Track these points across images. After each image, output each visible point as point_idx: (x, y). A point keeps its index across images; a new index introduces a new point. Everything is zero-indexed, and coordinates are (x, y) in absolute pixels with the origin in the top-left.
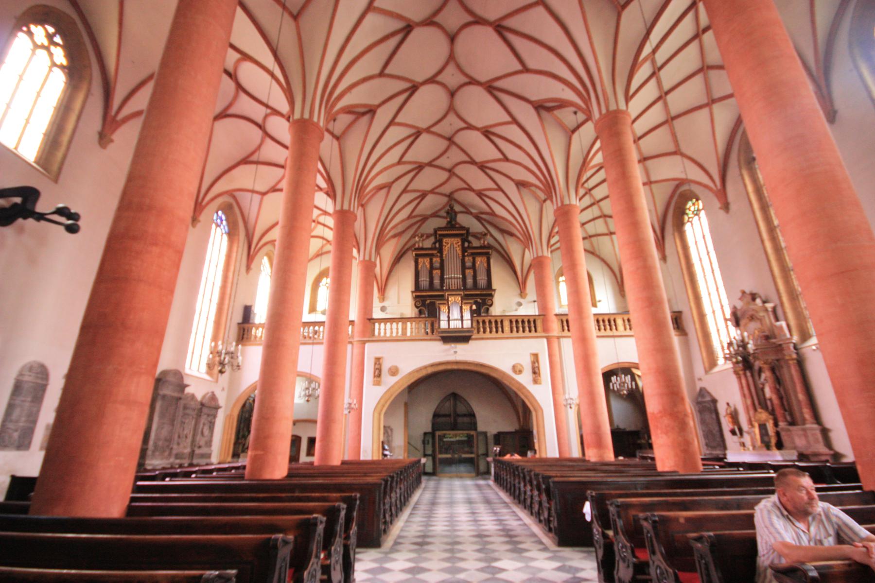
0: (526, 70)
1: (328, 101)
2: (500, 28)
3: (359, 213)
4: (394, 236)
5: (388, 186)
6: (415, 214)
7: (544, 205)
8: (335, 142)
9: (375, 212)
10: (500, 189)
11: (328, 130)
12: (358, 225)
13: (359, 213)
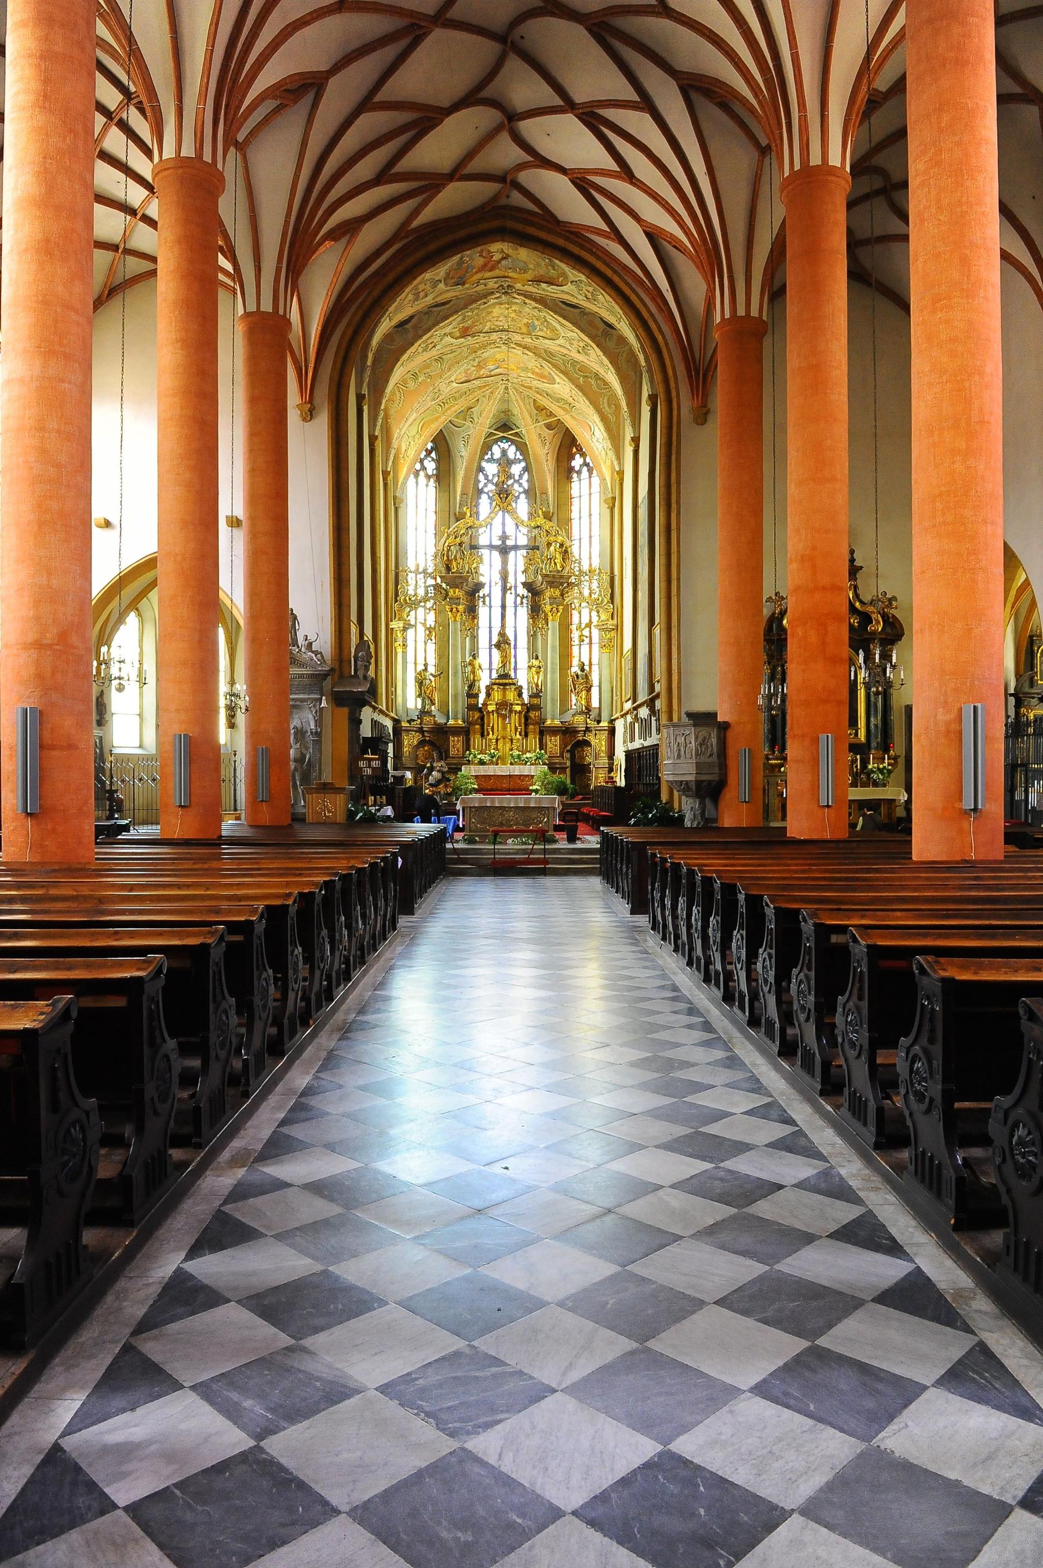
4: (335, 235)
6: (399, 168)
7: (767, 161)
9: (276, 166)
10: (647, 104)
12: (229, 208)
13: (230, 166)
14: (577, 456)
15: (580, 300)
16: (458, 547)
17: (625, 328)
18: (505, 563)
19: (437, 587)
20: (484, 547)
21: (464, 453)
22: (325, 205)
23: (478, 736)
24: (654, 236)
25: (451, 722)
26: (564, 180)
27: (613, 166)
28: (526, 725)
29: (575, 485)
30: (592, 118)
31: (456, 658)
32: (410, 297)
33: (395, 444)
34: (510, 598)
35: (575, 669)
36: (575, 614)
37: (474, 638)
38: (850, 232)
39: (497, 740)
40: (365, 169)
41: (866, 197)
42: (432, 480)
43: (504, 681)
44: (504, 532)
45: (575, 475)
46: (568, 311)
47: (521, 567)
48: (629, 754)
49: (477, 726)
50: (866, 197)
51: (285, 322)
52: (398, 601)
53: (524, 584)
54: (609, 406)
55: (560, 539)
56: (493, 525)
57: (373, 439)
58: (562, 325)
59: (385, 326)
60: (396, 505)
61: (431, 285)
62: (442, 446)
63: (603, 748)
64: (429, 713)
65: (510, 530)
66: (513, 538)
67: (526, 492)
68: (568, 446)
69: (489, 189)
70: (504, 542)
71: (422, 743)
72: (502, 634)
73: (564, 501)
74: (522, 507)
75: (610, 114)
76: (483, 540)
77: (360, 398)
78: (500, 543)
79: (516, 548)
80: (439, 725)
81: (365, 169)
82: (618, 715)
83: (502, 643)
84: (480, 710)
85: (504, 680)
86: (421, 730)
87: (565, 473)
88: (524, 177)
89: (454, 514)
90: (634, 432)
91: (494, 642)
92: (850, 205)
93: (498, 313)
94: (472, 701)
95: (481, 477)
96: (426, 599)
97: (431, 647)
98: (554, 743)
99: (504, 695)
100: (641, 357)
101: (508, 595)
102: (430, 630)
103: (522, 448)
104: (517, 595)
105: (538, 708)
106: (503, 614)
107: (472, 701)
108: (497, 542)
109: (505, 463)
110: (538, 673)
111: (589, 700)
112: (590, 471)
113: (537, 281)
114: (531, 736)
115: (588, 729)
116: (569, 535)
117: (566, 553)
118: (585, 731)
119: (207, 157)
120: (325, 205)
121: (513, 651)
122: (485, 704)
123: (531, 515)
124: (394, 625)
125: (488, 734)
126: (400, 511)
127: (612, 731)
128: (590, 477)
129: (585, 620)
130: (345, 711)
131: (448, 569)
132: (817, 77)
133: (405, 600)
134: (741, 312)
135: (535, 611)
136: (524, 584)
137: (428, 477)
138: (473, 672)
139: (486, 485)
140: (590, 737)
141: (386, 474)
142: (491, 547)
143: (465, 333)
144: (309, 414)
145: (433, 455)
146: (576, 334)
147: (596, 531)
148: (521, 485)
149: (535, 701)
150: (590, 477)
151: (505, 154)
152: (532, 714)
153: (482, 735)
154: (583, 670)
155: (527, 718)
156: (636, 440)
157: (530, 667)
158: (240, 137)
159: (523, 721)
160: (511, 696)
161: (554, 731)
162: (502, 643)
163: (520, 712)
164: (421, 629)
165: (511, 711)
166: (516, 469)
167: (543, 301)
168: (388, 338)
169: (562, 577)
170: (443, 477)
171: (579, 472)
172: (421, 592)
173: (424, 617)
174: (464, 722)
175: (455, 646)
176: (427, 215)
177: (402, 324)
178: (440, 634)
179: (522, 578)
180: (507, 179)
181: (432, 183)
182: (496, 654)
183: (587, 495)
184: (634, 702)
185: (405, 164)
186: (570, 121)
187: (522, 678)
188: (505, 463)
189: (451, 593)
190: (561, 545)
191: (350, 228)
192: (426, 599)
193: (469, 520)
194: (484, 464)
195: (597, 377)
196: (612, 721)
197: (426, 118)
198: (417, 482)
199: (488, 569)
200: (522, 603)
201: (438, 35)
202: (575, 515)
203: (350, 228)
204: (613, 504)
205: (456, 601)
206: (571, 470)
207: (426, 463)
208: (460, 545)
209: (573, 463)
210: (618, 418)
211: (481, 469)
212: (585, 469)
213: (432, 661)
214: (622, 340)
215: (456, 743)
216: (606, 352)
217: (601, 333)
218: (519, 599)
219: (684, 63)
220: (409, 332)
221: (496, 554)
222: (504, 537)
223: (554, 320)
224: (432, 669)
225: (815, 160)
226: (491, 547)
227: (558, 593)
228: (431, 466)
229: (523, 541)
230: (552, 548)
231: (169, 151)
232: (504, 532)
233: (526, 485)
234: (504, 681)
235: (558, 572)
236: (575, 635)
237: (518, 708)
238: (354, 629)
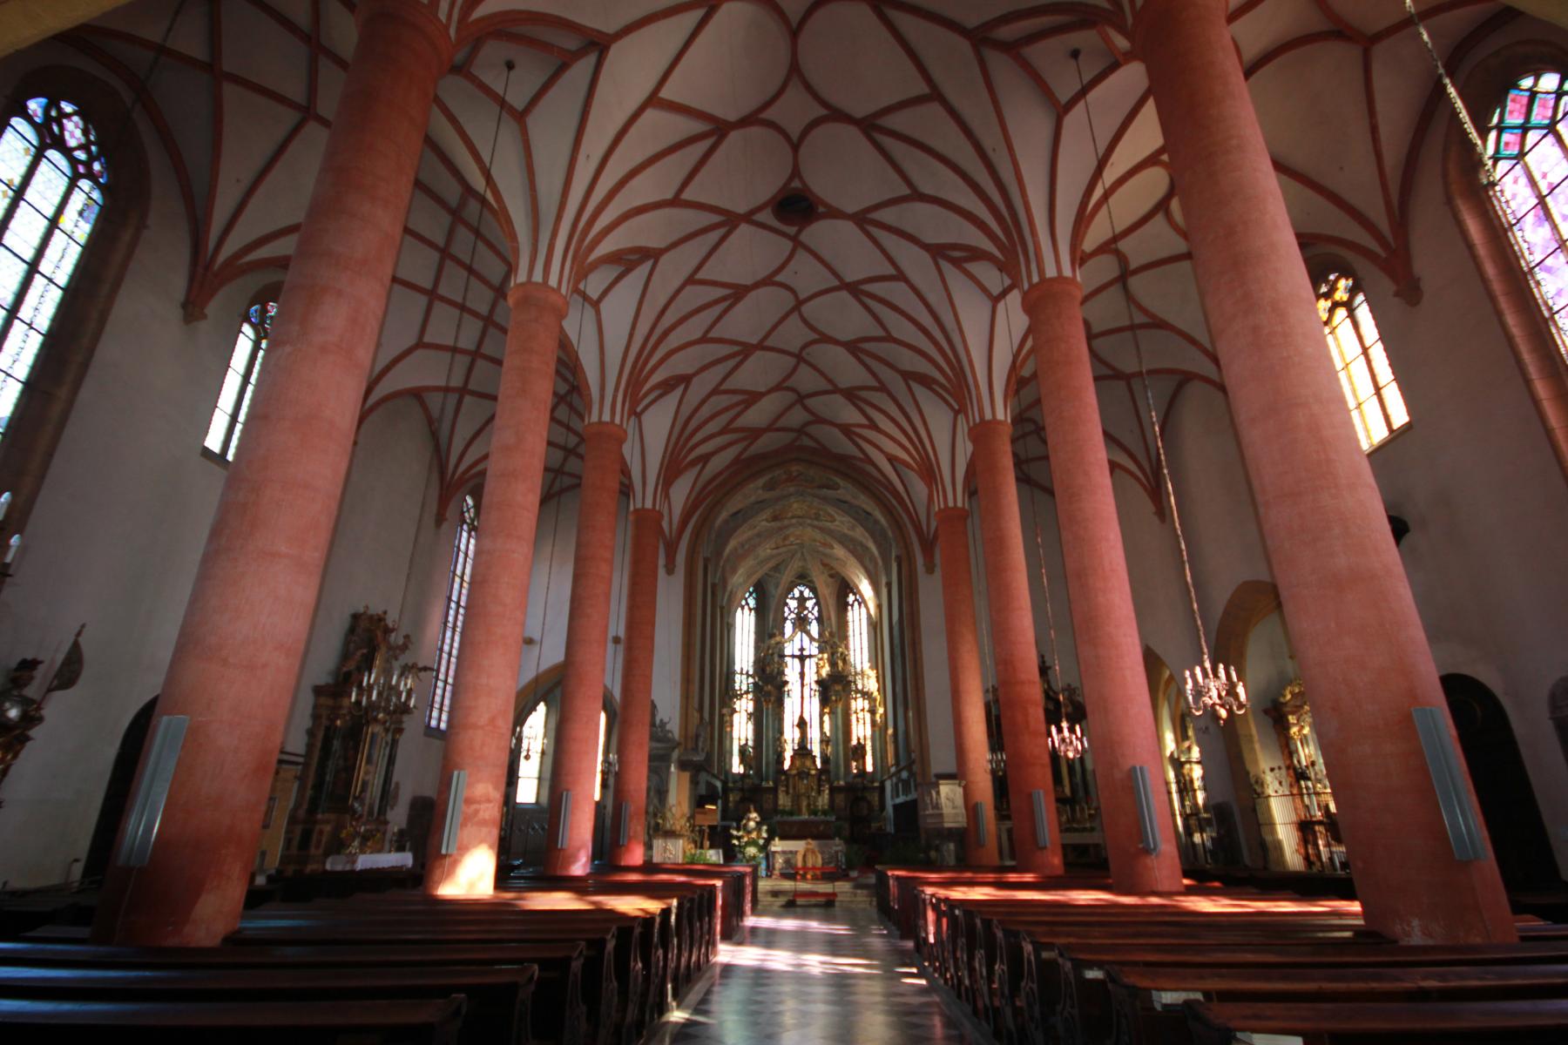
0: (918, 196)
1: (582, 240)
2: (869, 126)
3: (631, 427)
4: (693, 463)
5: (685, 380)
8: (589, 312)
10: (883, 388)
11: (576, 290)
13: (631, 427)
15: (848, 498)
17: (878, 515)
19: (755, 684)
21: (775, 593)
22: (691, 444)
24: (892, 459)
26: (836, 431)
27: (864, 421)
29: (850, 614)
30: (851, 395)
31: (769, 734)
34: (806, 690)
35: (854, 742)
38: (1015, 455)
40: (712, 427)
41: (1024, 436)
46: (840, 504)
47: (814, 669)
48: (895, 807)
50: (1024, 436)
51: (661, 515)
52: (729, 695)
53: (817, 682)
56: (794, 642)
57: (714, 586)
59: (724, 515)
60: (729, 627)
61: (753, 491)
62: (761, 592)
68: (845, 588)
69: (793, 435)
73: (843, 624)
74: (814, 628)
75: (863, 394)
76: (788, 652)
77: (706, 561)
78: (797, 653)
79: (810, 656)
81: (712, 427)
83: (802, 724)
85: (803, 751)
86: (742, 790)
87: (843, 607)
88: (812, 429)
89: (768, 634)
92: (1014, 441)
93: (797, 507)
96: (747, 692)
97: (751, 726)
100: (890, 534)
102: (750, 715)
103: (813, 590)
106: (801, 703)
108: (797, 653)
109: (802, 600)
113: (821, 487)
115: (865, 788)
116: (847, 647)
117: (845, 661)
119: (617, 421)
120: (691, 444)
123: (820, 634)
124: (725, 711)
127: (882, 789)
130: (687, 775)
131: (763, 670)
132: (985, 372)
134: (951, 504)
135: (825, 701)
136: (817, 682)
140: (868, 795)
141: (722, 608)
142: (793, 656)
143: (775, 518)
144: (670, 570)
146: (846, 519)
151: (797, 417)
155: (819, 780)
156: (889, 585)
158: (639, 409)
160: (808, 763)
161: (840, 789)
162: (802, 724)
164: (744, 715)
166: (810, 604)
167: (825, 499)
168: (726, 522)
170: (760, 612)
172: (744, 688)
173: (744, 706)
176: (753, 450)
177: (736, 513)
178: (757, 717)
180: (801, 431)
181: (755, 433)
182: (797, 731)
183: (858, 621)
185: (739, 423)
186: (839, 399)
187: (816, 751)
188: (802, 600)
191: (705, 459)
192: (747, 692)
193: (778, 639)
195: (862, 545)
197: (753, 398)
199: (791, 671)
201: (759, 353)
202: (850, 633)
203: (705, 459)
204: (874, 626)
205: (769, 694)
206: (847, 604)
213: (750, 736)
214: (876, 522)
216: (867, 530)
217: (863, 518)
219: (908, 367)
220: (740, 517)
221: (797, 661)
222: (802, 649)
223: (831, 510)
224: (750, 743)
225: (988, 416)
226: (793, 656)
228: (752, 602)
229: (815, 651)
231: (594, 418)
236: (854, 718)
238: (696, 715)
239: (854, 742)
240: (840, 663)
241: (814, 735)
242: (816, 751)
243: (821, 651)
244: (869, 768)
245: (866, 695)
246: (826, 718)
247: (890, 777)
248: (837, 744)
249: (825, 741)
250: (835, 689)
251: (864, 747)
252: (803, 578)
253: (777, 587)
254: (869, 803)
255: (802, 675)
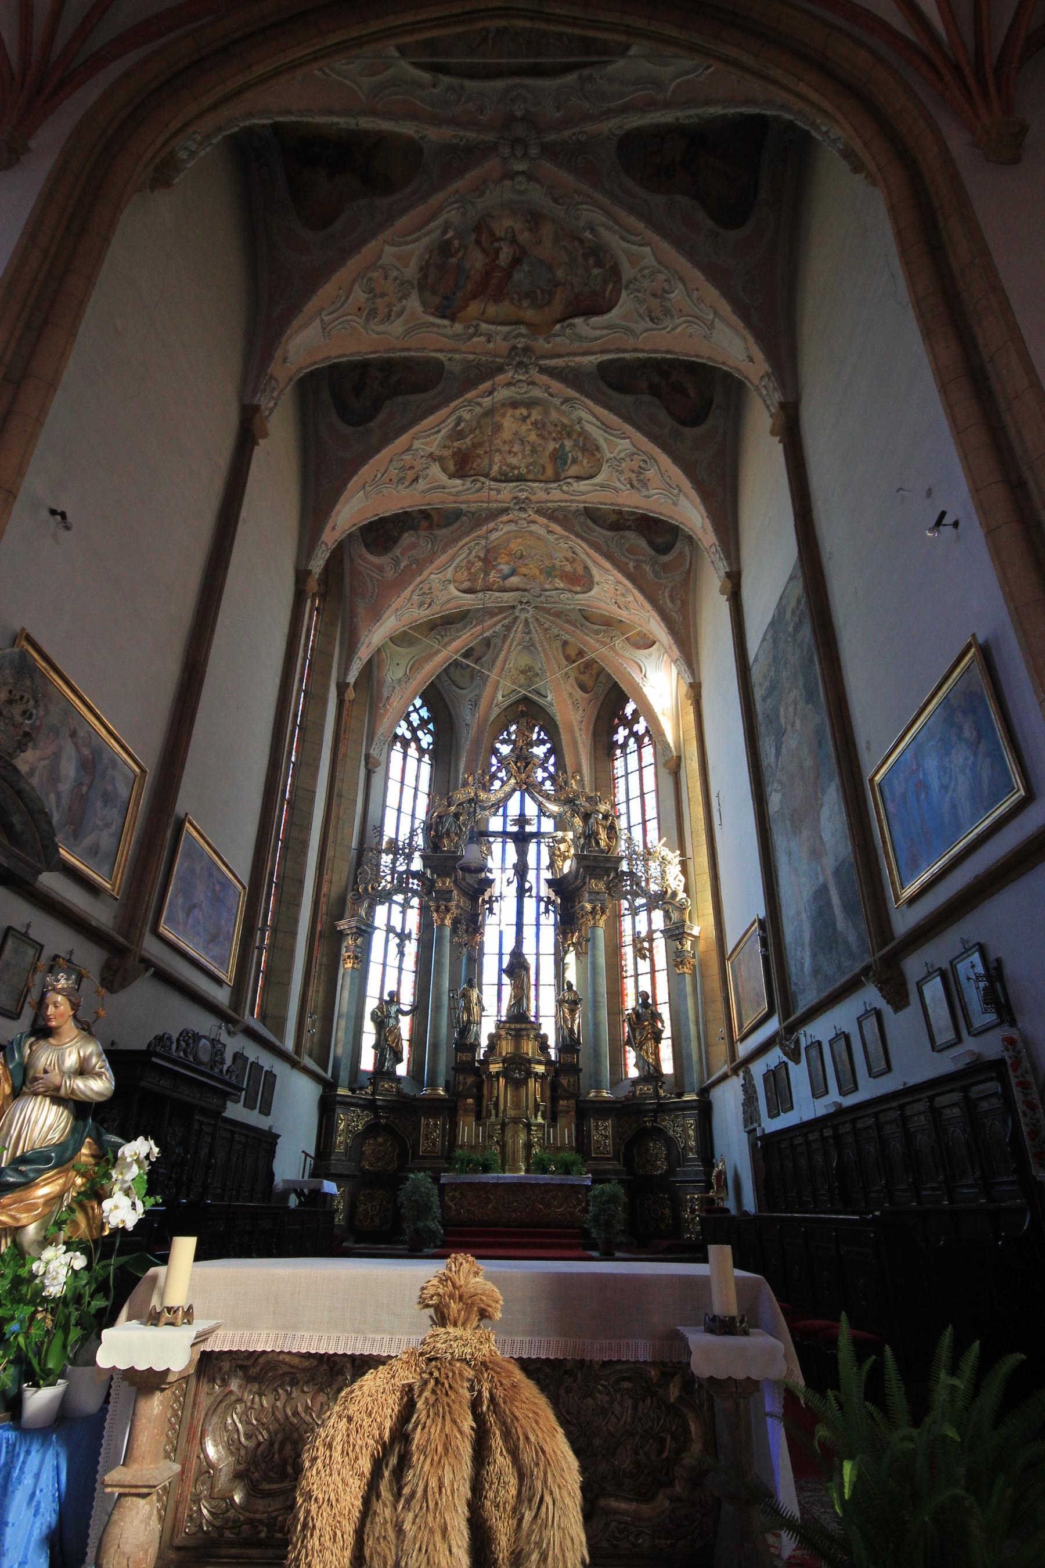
14: (621, 729)
16: (451, 819)
18: (522, 853)
20: (495, 834)
21: (470, 720)
23: (471, 1119)
25: (426, 1091)
28: (554, 1100)
29: (619, 764)
32: (359, 295)
33: (364, 653)
34: (529, 904)
35: (630, 1002)
36: (627, 923)
37: (475, 961)
39: (503, 1125)
42: (427, 756)
43: (518, 1026)
44: (522, 815)
45: (618, 752)
47: (545, 861)
48: (767, 1149)
49: (470, 1101)
53: (550, 883)
54: (672, 601)
55: (603, 808)
58: (606, 427)
63: (692, 1143)
64: (391, 1075)
65: (531, 809)
66: (535, 821)
67: (552, 777)
70: (522, 827)
71: (371, 1130)
72: (517, 954)
76: (495, 824)
78: (515, 829)
80: (406, 1096)
82: (725, 1068)
84: (477, 1072)
85: (518, 1021)
86: (370, 1105)
87: (605, 750)
90: (730, 564)
91: (504, 966)
94: (465, 1057)
95: (494, 761)
98: (603, 1133)
99: (518, 1046)
101: (526, 900)
104: (539, 899)
105: (574, 1070)
107: (465, 1057)
110: (572, 1012)
111: (656, 1053)
112: (639, 740)
114: (561, 1122)
115: (662, 1108)
117: (612, 830)
118: (656, 1112)
121: (533, 988)
122: (485, 1063)
125: (489, 1117)
126: (377, 780)
127: (705, 1110)
128: (640, 748)
129: (643, 928)
133: (366, 889)
135: (568, 923)
136: (550, 883)
137: (421, 751)
138: (468, 1009)
139: (499, 769)
140: (666, 1123)
145: (431, 726)
147: (651, 812)
148: (545, 769)
149: (568, 1058)
150: (640, 748)
152: (564, 1082)
153: (479, 1117)
154: (645, 1005)
155: (555, 1086)
157: (560, 1003)
159: (548, 1093)
160: (529, 1048)
161: (603, 1109)
162: (517, 968)
163: (543, 1077)
165: (529, 1073)
166: (540, 751)
169: (608, 859)
171: (624, 746)
174: (446, 1090)
175: (439, 963)
179: (547, 875)
182: (506, 979)
184: (786, 1015)
187: (548, 1028)
189: (439, 884)
190: (606, 817)
194: (498, 745)
196: (704, 1092)
198: (405, 755)
199: (499, 861)
200: (547, 911)
207: (420, 734)
208: (457, 816)
209: (615, 737)
210: (685, 617)
211: (495, 752)
212: (632, 740)
215: (431, 1132)
218: (542, 905)
222: (522, 820)
226: (504, 834)
227: (601, 886)
228: (426, 740)
230: (592, 820)
232: (522, 815)
233: (552, 769)
234: (518, 1026)
235: (602, 851)
236: (628, 952)
237: (540, 1069)
239: (630, 1002)
240: (603, 835)
241: (545, 1007)
242: (548, 1028)
243: (561, 824)
244: (667, 1067)
245: (661, 900)
246: (571, 958)
247: (741, 1066)
248: (595, 1007)
249: (568, 1001)
250: (593, 885)
251: (656, 1016)
252: (528, 711)
253: (475, 704)
254: (670, 1143)
255: (521, 870)
